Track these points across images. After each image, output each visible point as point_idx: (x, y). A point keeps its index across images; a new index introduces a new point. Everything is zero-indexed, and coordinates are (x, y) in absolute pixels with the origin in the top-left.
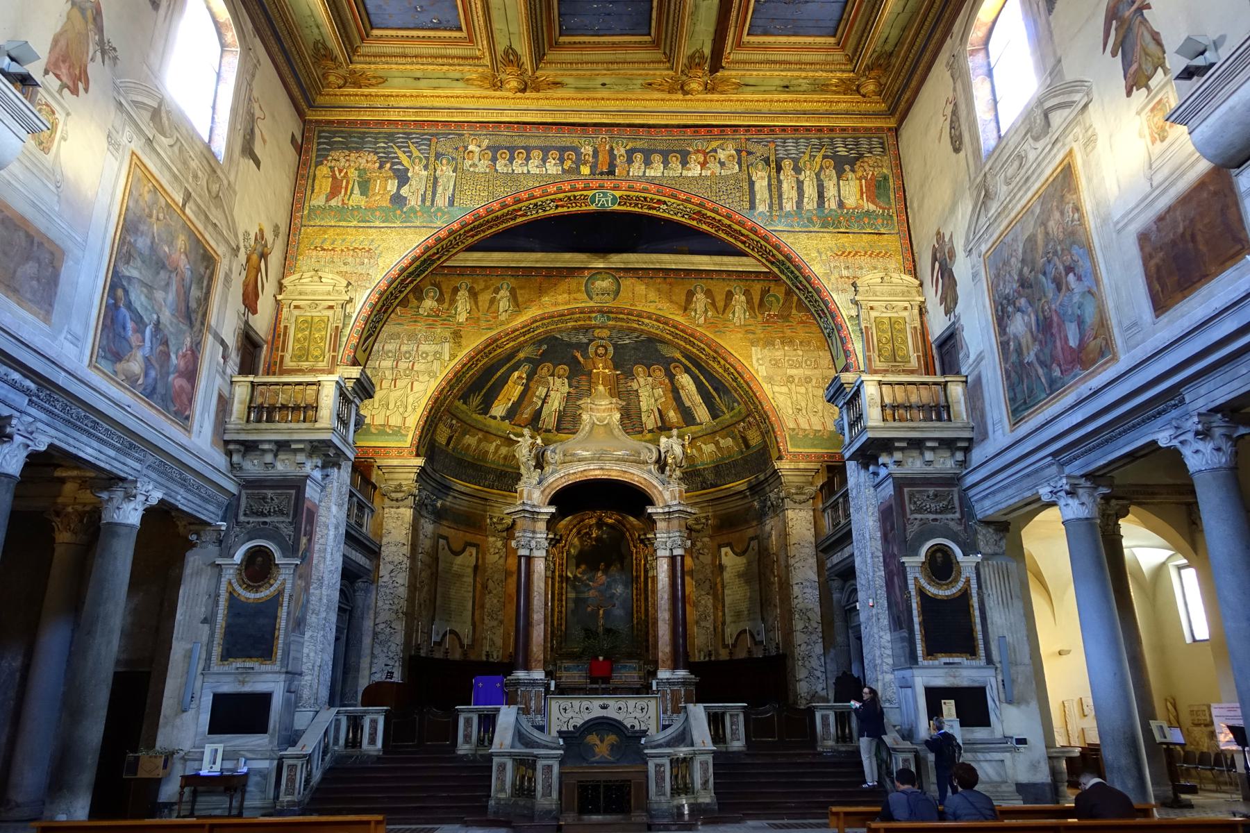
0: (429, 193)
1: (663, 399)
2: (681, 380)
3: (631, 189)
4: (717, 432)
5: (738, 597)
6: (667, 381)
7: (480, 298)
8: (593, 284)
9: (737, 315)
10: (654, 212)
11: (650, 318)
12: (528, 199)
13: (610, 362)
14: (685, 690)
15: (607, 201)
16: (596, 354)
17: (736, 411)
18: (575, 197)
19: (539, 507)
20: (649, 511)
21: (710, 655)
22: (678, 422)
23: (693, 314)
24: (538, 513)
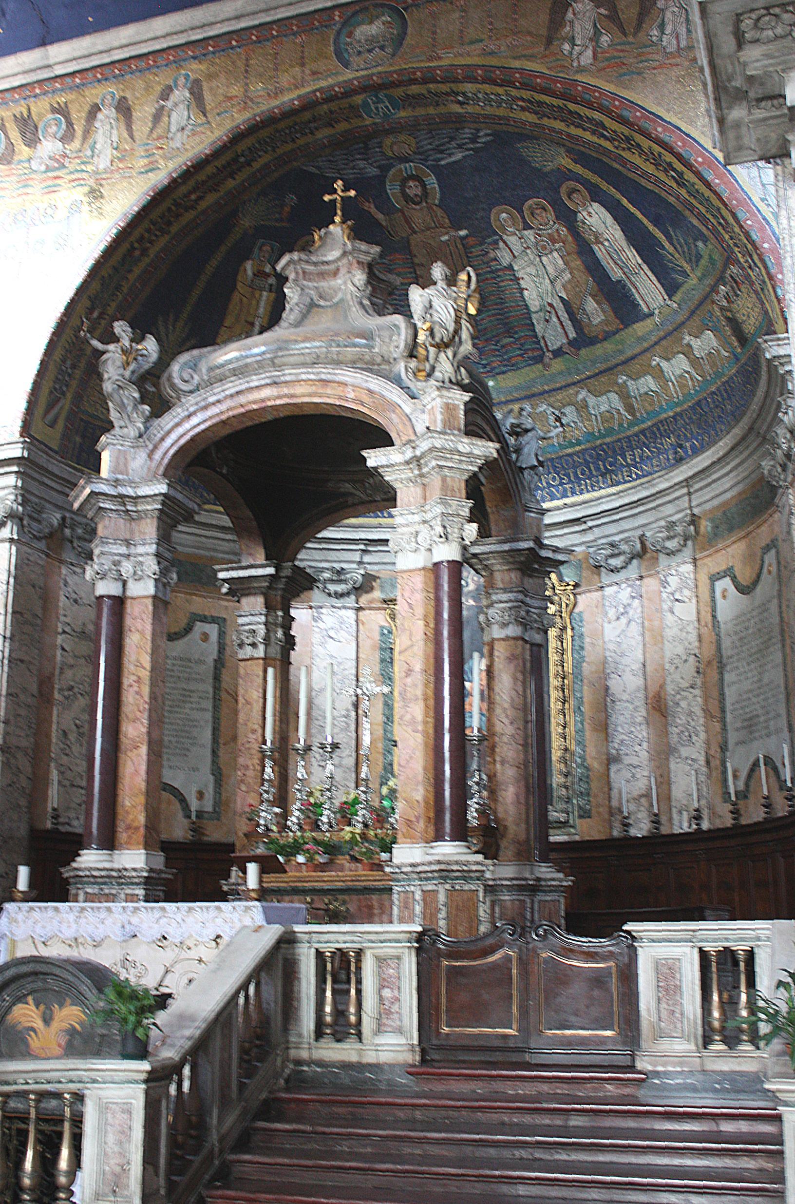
1: (567, 276)
2: (589, 221)
4: (683, 323)
5: (747, 685)
6: (564, 231)
7: (136, 114)
8: (350, 34)
9: (669, 29)
11: (473, 80)
13: (439, 212)
14: (450, 893)
16: (407, 198)
17: (703, 262)
19: (131, 483)
20: (370, 463)
21: (698, 818)
22: (606, 322)
23: (567, 47)
24: (136, 499)
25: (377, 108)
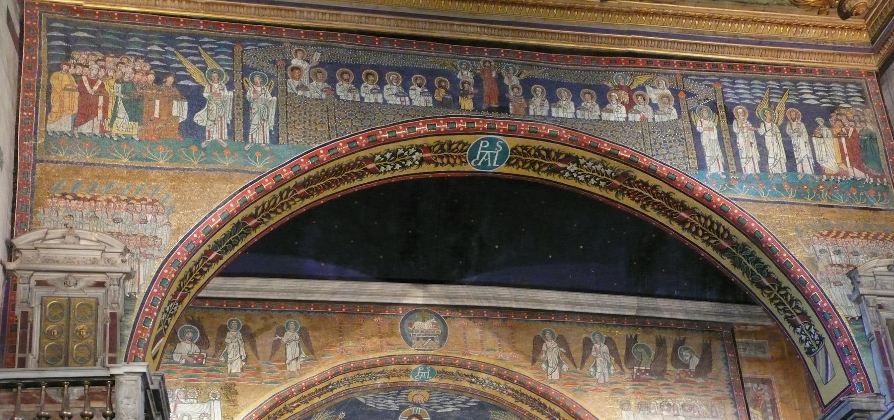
0: (239, 123)
3: (532, 135)
8: (411, 325)
10: (555, 178)
12: (388, 142)
15: (493, 155)
18: (450, 144)
25: (420, 374)
